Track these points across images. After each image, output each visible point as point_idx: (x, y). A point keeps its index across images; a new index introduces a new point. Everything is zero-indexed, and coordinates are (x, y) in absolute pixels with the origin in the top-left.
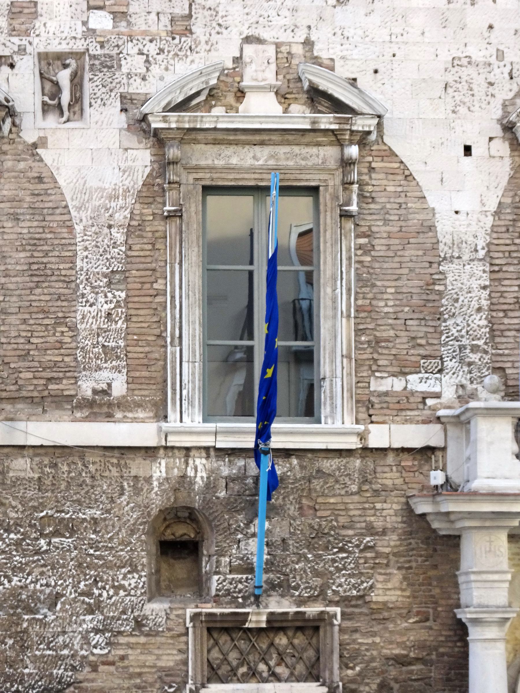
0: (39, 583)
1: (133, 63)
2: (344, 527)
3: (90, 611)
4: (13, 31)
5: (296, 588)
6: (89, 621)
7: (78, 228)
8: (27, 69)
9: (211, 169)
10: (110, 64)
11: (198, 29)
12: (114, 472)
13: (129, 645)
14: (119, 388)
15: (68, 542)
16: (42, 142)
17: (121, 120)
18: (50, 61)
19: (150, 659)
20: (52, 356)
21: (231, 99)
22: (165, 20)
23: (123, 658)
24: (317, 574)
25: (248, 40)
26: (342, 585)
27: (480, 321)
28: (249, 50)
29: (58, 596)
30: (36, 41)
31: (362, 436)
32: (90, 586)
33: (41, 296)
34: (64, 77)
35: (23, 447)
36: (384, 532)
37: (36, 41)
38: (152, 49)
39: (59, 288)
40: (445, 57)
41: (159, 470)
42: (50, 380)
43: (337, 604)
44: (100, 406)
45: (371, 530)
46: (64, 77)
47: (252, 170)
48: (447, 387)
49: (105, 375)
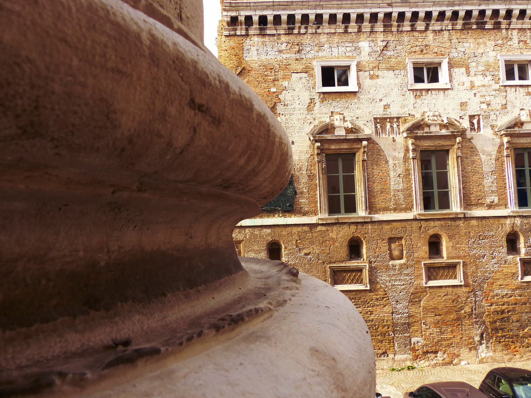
0: (481, 252)
1: (493, 117)
3: (493, 259)
4: (462, 110)
7: (483, 160)
8: (467, 118)
9: (516, 143)
10: (487, 117)
11: (508, 107)
12: (497, 222)
14: (496, 200)
15: (486, 241)
16: (472, 138)
17: (492, 132)
18: (472, 117)
19: (510, 271)
20: (479, 193)
21: (519, 125)
22: (500, 105)
25: (521, 110)
28: (522, 112)
29: (485, 255)
30: (468, 112)
34: (475, 121)
35: (473, 217)
37: (468, 112)
38: (498, 113)
39: (479, 176)
41: (508, 221)
42: (479, 199)
46: (475, 121)
47: (526, 143)
49: (492, 197)
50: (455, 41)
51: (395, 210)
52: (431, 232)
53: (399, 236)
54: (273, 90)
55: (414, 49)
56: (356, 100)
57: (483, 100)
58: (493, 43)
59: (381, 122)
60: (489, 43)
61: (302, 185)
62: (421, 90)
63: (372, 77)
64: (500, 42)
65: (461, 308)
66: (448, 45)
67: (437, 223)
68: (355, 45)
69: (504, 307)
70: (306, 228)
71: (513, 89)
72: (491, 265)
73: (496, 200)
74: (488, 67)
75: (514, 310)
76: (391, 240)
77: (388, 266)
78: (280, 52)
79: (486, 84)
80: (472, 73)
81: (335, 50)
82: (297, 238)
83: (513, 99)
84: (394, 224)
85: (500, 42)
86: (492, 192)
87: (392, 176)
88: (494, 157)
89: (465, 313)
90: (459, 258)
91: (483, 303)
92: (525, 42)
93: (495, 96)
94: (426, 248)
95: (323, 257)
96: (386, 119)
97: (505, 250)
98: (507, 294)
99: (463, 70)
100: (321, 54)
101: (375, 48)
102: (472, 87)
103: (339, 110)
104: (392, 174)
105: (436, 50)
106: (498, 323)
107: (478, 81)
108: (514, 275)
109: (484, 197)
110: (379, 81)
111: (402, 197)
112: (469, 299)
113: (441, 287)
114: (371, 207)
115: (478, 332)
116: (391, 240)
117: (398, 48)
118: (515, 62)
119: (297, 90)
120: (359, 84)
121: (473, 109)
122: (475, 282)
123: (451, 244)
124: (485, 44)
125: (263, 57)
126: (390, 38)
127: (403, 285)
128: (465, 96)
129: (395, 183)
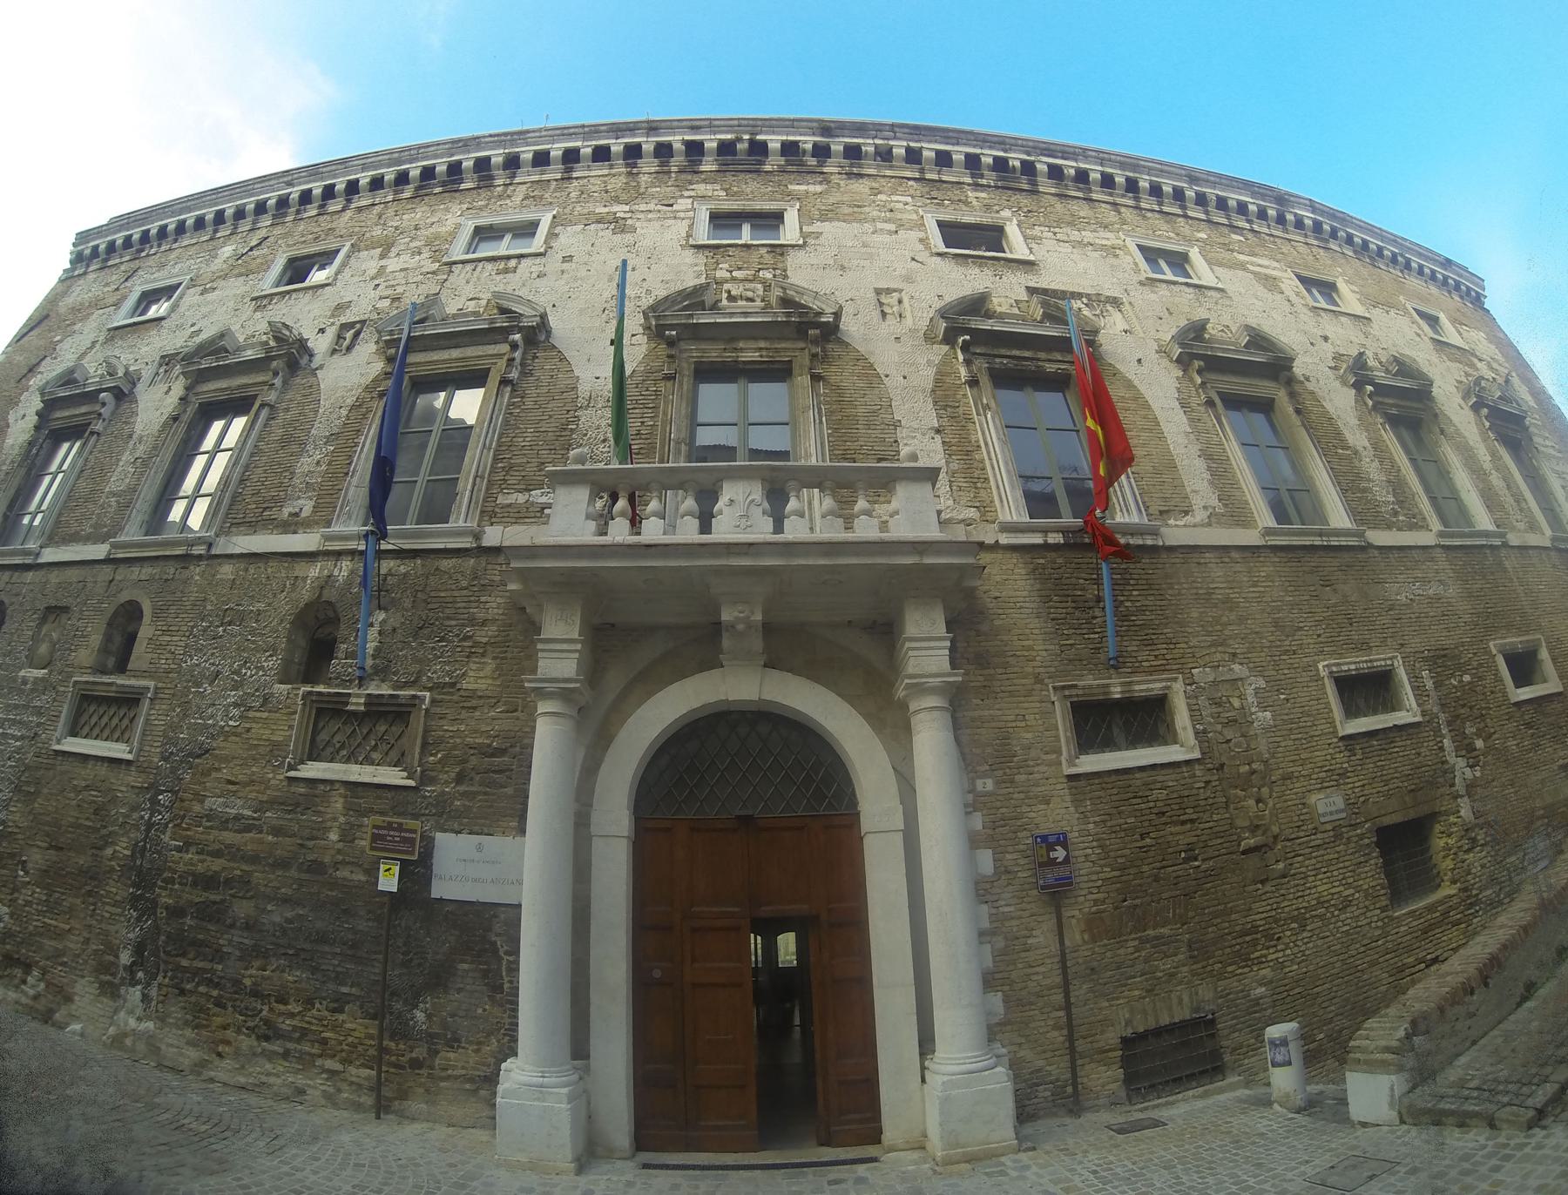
2: (449, 618)
3: (235, 688)
5: (395, 674)
6: (233, 696)
13: (254, 720)
23: (248, 730)
24: (416, 660)
26: (437, 672)
31: (477, 536)
32: (241, 667)
36: (484, 623)
41: (315, 571)
43: (430, 689)
45: (472, 621)
65: (107, 841)
67: (147, 571)
69: (217, 865)
75: (245, 881)
77: (14, 680)
89: (113, 857)
91: (166, 838)
97: (272, 663)
98: (238, 818)
106: (188, 921)
108: (276, 748)
112: (135, 815)
113: (85, 758)
115: (131, 936)
122: (165, 759)
127: (22, 738)
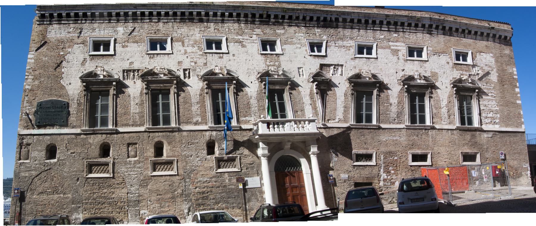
1: (198, 70)
4: (179, 66)
8: (182, 71)
10: (195, 70)
11: (208, 64)
14: (200, 120)
17: (197, 78)
18: (185, 70)
20: (189, 116)
27: (256, 108)
33: (186, 106)
34: (187, 72)
39: (189, 105)
40: (246, 69)
41: (208, 133)
44: (196, 124)
48: (252, 119)
50: (176, 28)
51: (133, 125)
52: (156, 140)
53: (134, 142)
54: (62, 53)
55: (150, 32)
56: (112, 60)
57: (192, 60)
58: (199, 29)
59: (126, 72)
60: (196, 29)
61: (73, 109)
62: (154, 54)
63: (123, 47)
64: (203, 29)
66: (171, 29)
67: (160, 134)
68: (115, 29)
70: (73, 136)
71: (211, 55)
72: (196, 161)
73: (200, 120)
74: (196, 42)
76: (129, 145)
77: (126, 161)
78: (69, 32)
79: (194, 51)
80: (186, 45)
81: (102, 32)
82: (67, 143)
83: (211, 60)
84: (132, 134)
85: (203, 29)
86: (197, 115)
87: (132, 104)
88: (198, 93)
90: (174, 157)
92: (218, 30)
93: (200, 58)
94: (152, 150)
95: (83, 155)
96: (130, 71)
99: (180, 43)
100: (93, 34)
101: (127, 31)
102: (186, 53)
103: (101, 65)
104: (132, 103)
105: (164, 32)
107: (189, 49)
109: (192, 118)
110: (128, 49)
111: (138, 117)
114: (116, 124)
116: (129, 145)
117: (141, 31)
118: (213, 40)
119: (76, 53)
120: (115, 50)
121: (186, 65)
123: (169, 148)
124: (194, 30)
125: (58, 36)
126: (136, 25)
128: (181, 58)
129: (134, 109)
